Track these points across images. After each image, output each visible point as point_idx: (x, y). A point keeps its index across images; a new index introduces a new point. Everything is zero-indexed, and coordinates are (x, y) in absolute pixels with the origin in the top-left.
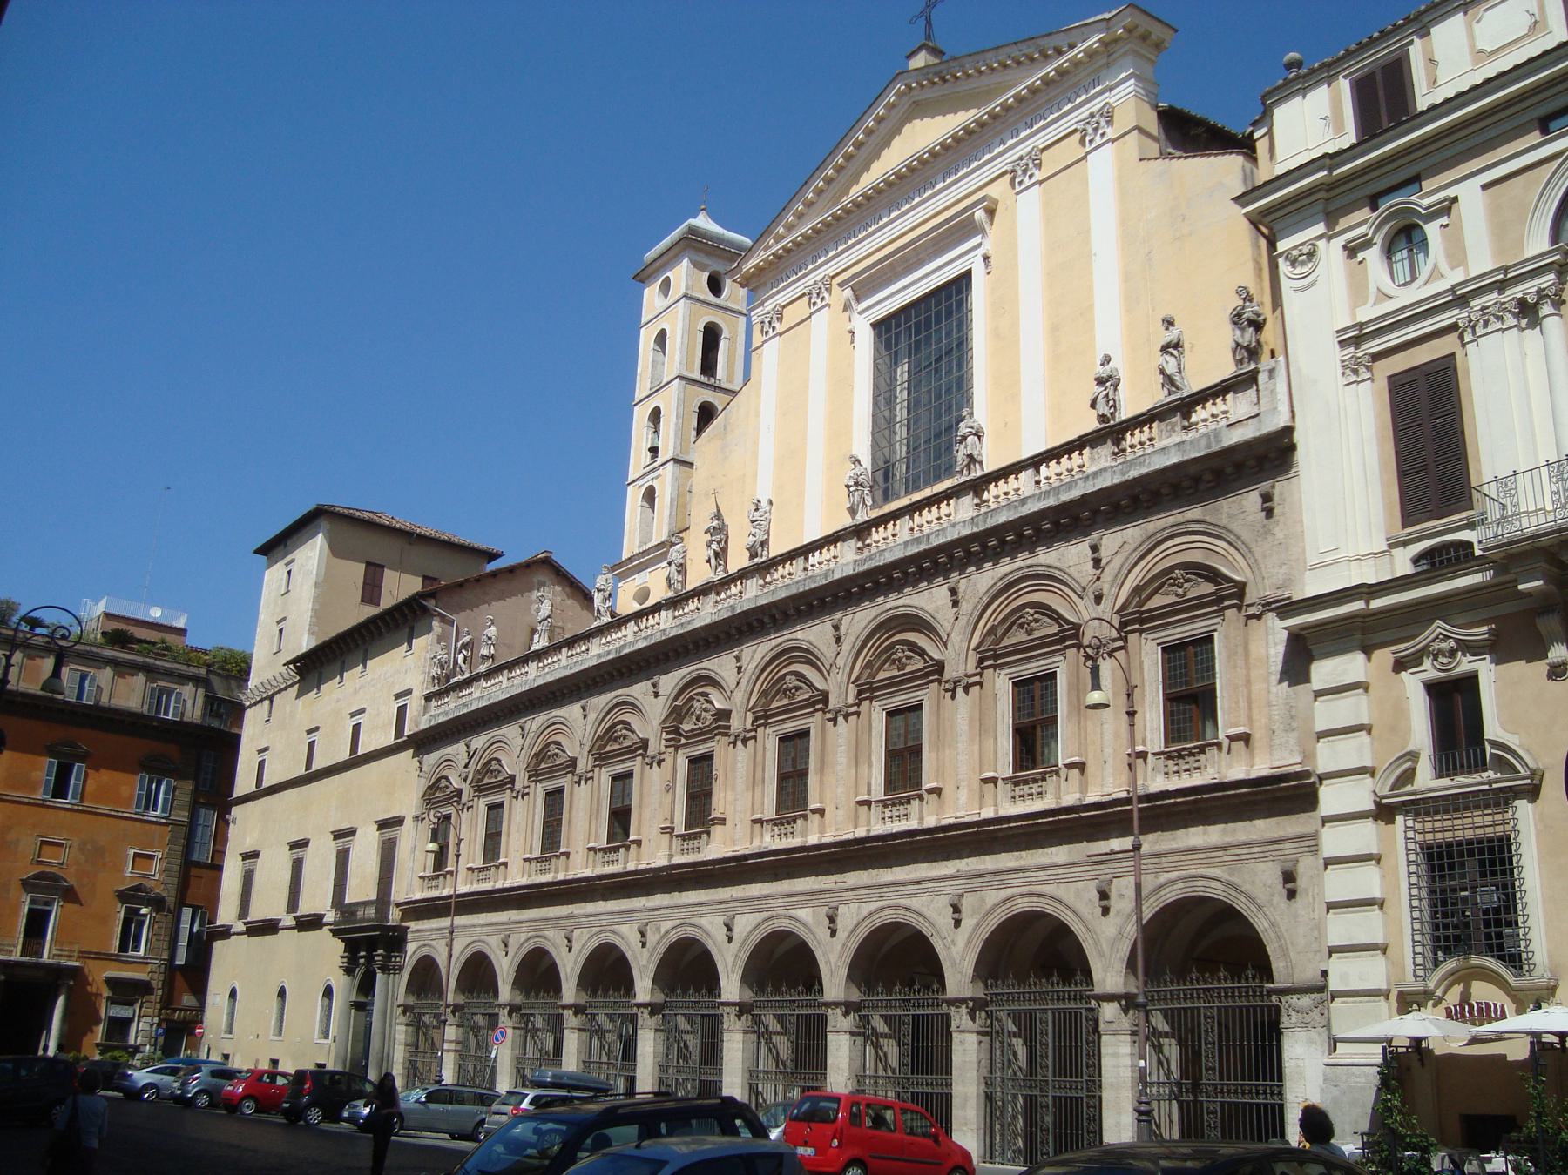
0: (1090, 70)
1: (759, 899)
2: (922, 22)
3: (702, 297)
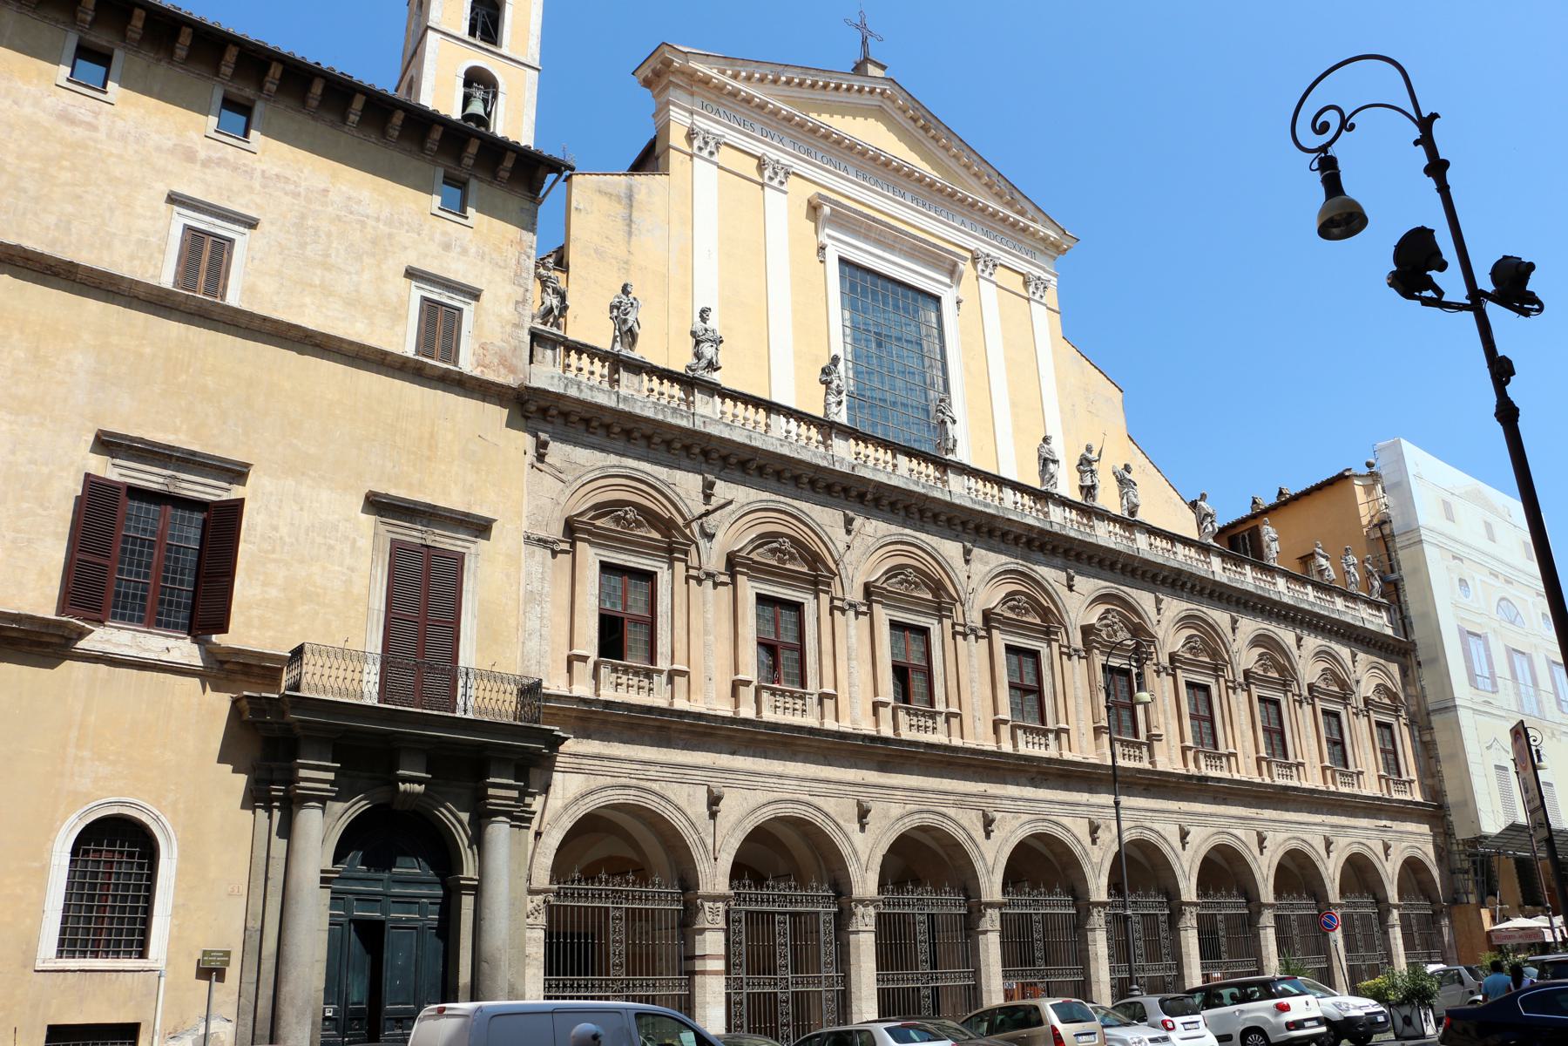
0: (1032, 243)
1: (1206, 815)
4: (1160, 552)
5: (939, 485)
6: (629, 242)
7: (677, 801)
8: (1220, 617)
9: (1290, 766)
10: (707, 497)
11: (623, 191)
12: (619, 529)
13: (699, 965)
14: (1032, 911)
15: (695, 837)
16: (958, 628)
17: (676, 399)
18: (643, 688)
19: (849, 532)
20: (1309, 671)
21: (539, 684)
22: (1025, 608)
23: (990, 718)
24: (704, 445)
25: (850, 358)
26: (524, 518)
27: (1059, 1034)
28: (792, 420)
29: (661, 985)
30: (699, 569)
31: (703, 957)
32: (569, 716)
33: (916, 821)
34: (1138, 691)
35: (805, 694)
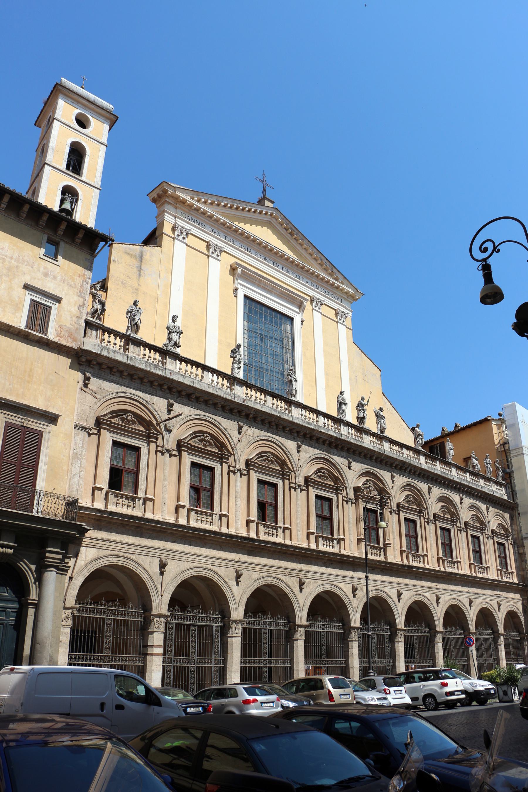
0: (341, 295)
1: (411, 585)
4: (395, 452)
5: (287, 412)
6: (139, 279)
7: (143, 565)
8: (423, 486)
9: (454, 563)
10: (169, 411)
11: (138, 253)
12: (123, 424)
13: (149, 650)
14: (321, 630)
15: (152, 584)
16: (292, 485)
17: (157, 360)
18: (130, 506)
19: (240, 433)
20: (465, 515)
21: (76, 501)
22: (326, 477)
23: (305, 531)
24: (169, 385)
25: (246, 345)
26: (75, 415)
27: (332, 694)
28: (215, 375)
29: (129, 660)
30: (163, 447)
31: (152, 646)
32: (92, 518)
33: (265, 581)
34: (381, 521)
35: (213, 514)
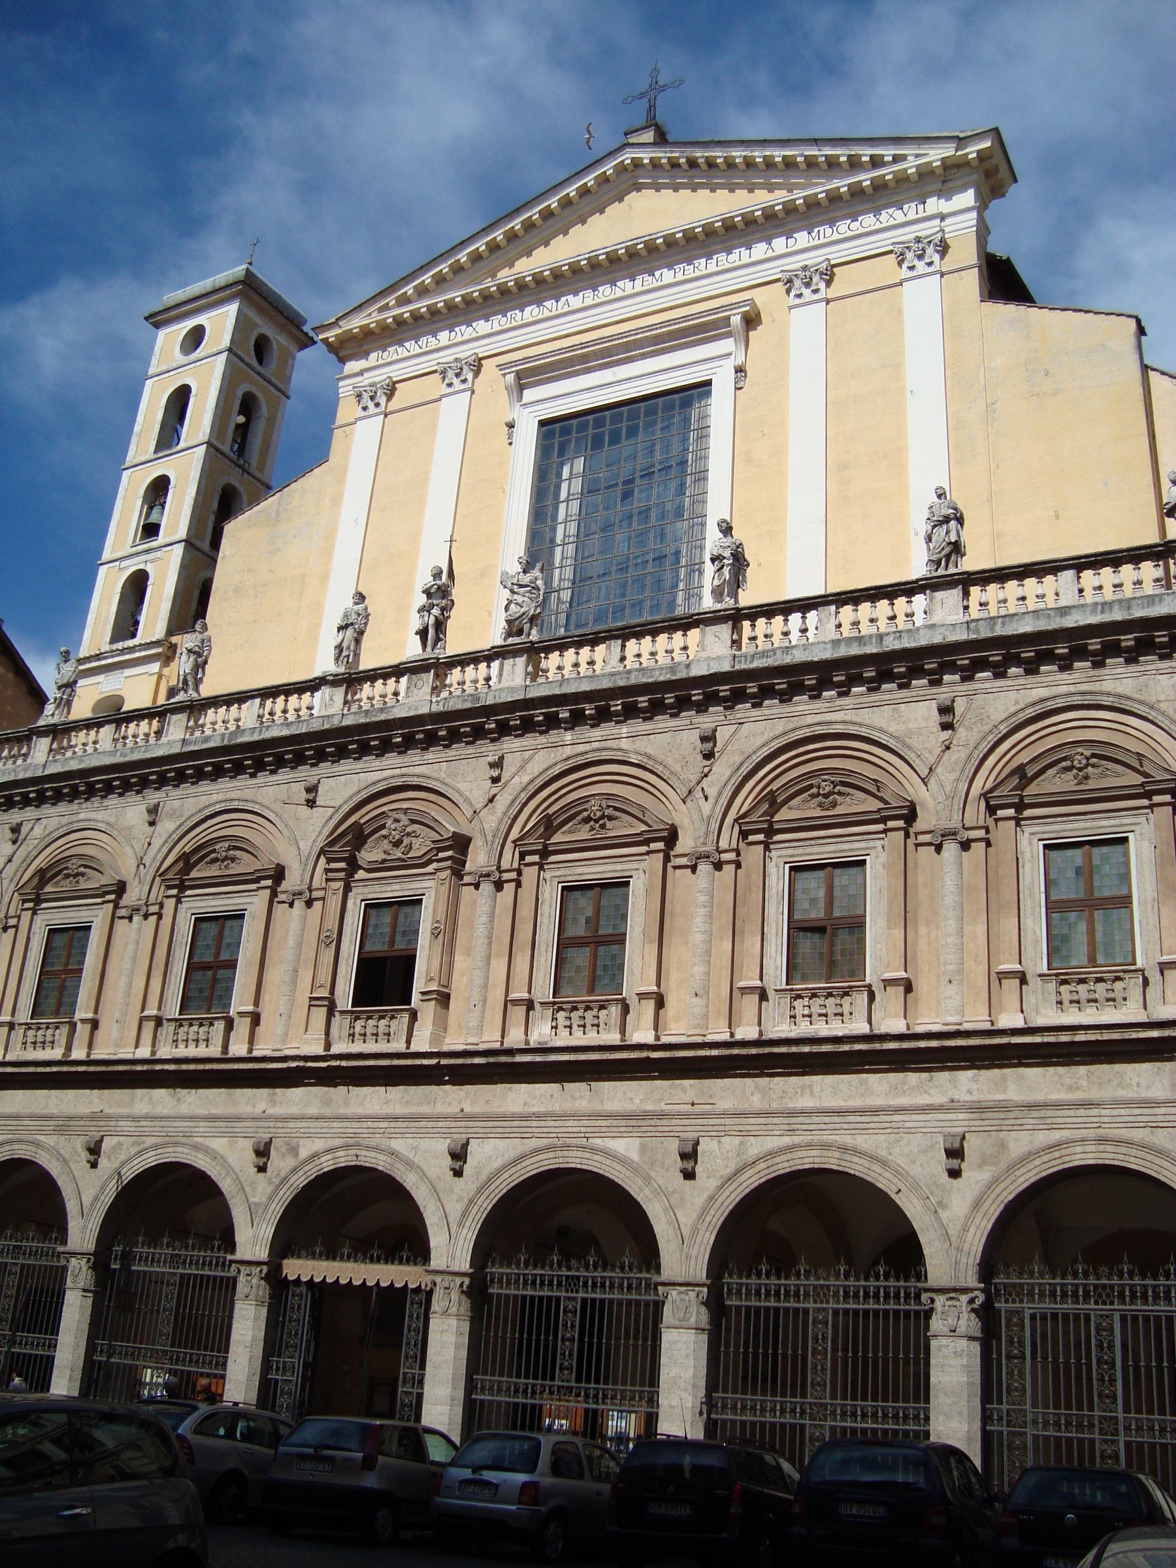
2: (644, 103)
3: (246, 358)
